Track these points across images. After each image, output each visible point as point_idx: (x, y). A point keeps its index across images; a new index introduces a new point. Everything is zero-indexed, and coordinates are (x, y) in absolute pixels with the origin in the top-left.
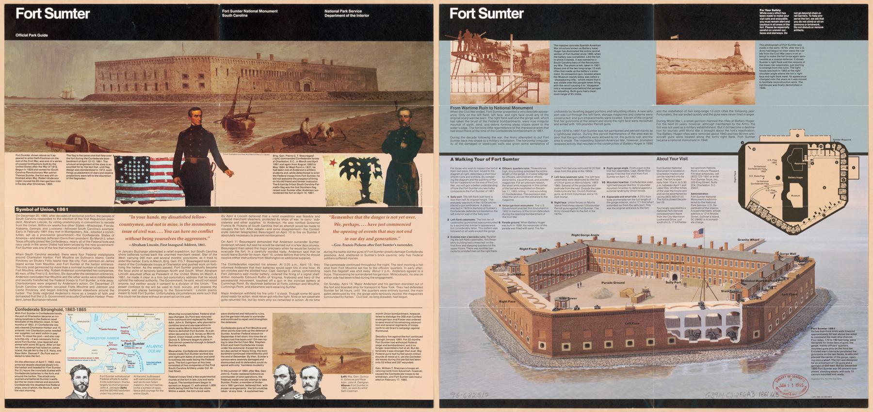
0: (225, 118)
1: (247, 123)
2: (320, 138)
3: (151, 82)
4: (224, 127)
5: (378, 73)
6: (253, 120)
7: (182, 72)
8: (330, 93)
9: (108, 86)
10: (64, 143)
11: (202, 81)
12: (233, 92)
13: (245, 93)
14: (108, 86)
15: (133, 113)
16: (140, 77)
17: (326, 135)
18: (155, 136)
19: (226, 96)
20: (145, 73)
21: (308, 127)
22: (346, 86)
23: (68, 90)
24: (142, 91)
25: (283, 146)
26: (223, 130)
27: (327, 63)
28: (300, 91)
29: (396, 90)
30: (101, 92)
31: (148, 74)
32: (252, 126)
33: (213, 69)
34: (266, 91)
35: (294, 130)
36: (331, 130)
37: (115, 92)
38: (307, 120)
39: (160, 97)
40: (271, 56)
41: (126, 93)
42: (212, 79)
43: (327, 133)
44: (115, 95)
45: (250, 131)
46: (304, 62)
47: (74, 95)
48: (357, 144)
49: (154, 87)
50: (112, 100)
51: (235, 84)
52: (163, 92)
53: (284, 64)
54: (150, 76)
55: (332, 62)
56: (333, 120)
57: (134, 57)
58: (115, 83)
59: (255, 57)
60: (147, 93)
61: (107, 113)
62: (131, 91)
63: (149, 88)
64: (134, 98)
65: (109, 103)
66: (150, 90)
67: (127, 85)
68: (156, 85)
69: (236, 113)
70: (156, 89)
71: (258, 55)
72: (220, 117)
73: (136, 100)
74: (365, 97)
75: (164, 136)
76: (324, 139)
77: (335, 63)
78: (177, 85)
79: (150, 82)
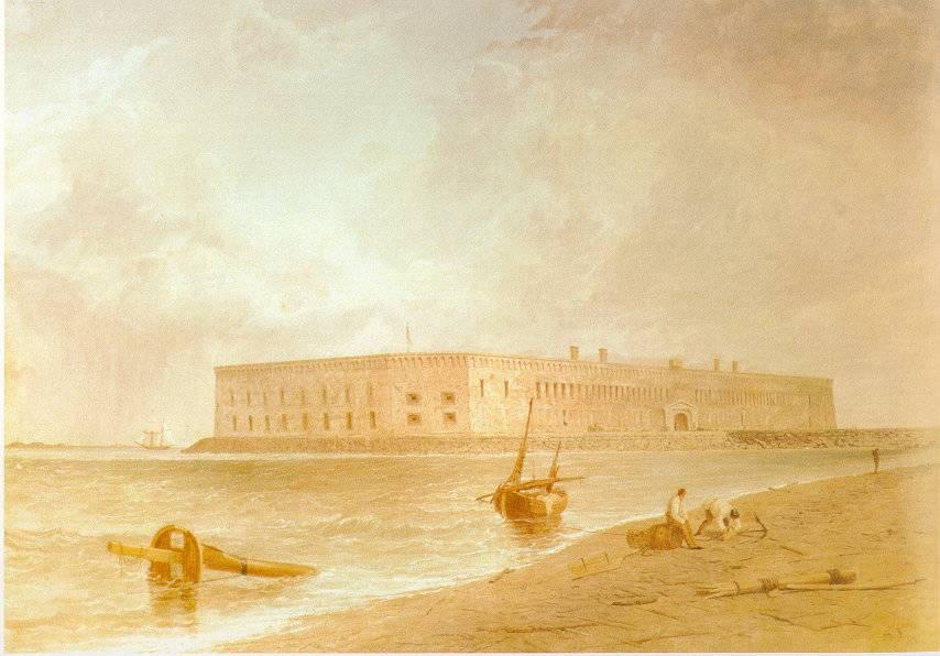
0: (500, 491)
1: (549, 501)
2: (709, 534)
3: (338, 411)
4: (498, 508)
5: (837, 390)
6: (562, 494)
7: (405, 389)
8: (732, 434)
9: (243, 420)
10: (147, 545)
11: (451, 409)
12: (519, 431)
13: (544, 436)
14: (243, 420)
15: (295, 479)
16: (315, 399)
17: (722, 526)
18: (346, 530)
19: (501, 442)
20: (325, 391)
21: (684, 511)
22: (766, 418)
23: (156, 428)
24: (318, 431)
25: (629, 551)
26: (498, 516)
27: (725, 367)
28: (665, 429)
29: (875, 426)
30: (228, 433)
31: (331, 393)
32: (559, 508)
33: (474, 381)
34: (591, 429)
35: (651, 516)
36: (734, 515)
37: (259, 432)
38: (681, 492)
39: (358, 444)
40: (602, 352)
41: (283, 434)
42: (472, 405)
43: (726, 521)
44: (259, 440)
45: (556, 518)
46: (674, 366)
47: (169, 438)
48: (790, 545)
49: (344, 422)
50: (250, 450)
51: (522, 416)
52: (364, 431)
53: (630, 370)
54: (335, 399)
55: (735, 365)
56: (738, 493)
57: (301, 355)
58: (258, 413)
59: (567, 355)
60: (329, 434)
61: (242, 477)
62: (294, 431)
63: (332, 423)
64: (301, 446)
65: (246, 457)
66: (337, 429)
67: (284, 417)
68: (349, 416)
69: (525, 478)
70: (350, 426)
71: (574, 350)
72: (493, 489)
73: (304, 450)
74: (808, 441)
75: (366, 528)
76: (718, 536)
77: (742, 368)
78: (395, 416)
79: (336, 412)
